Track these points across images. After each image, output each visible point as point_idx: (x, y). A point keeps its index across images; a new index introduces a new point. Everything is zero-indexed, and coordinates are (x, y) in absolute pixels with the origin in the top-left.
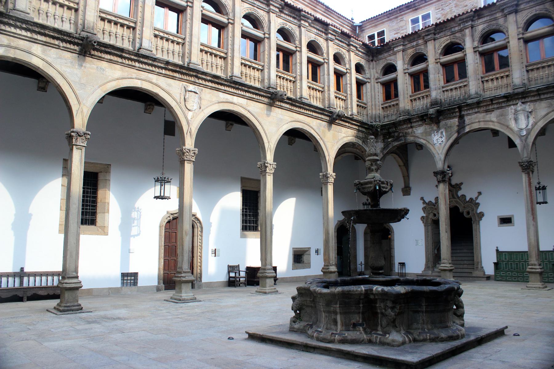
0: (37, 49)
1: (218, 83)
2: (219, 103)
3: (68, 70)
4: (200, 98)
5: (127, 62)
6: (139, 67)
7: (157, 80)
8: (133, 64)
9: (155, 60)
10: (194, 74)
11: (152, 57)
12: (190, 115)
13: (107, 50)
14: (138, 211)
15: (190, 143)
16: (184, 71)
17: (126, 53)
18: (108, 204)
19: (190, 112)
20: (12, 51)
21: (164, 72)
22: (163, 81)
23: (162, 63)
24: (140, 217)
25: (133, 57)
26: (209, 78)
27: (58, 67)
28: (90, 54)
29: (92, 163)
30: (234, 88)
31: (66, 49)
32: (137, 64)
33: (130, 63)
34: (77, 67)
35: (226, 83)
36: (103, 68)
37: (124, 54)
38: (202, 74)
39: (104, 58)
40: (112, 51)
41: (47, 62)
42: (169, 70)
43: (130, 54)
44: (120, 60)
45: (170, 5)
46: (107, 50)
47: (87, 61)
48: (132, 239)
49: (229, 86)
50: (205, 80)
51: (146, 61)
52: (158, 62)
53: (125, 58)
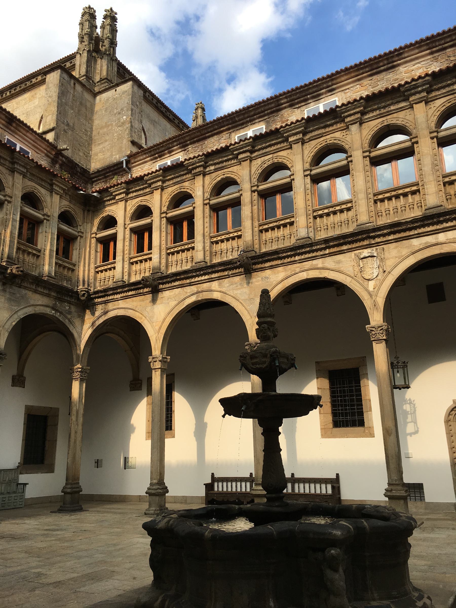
0: (215, 285)
1: (404, 231)
2: (413, 253)
3: (239, 292)
4: (382, 260)
5: (286, 260)
6: (300, 260)
7: (323, 263)
8: (293, 259)
9: (311, 245)
10: (364, 236)
11: (307, 244)
12: (371, 285)
13: (264, 259)
14: (410, 403)
15: (376, 318)
16: (349, 239)
17: (282, 253)
18: (370, 401)
19: (370, 282)
20: (201, 295)
21: (327, 251)
22: (329, 262)
23: (321, 244)
24: (415, 411)
25: (289, 253)
26: (385, 231)
27: (231, 293)
28: (253, 270)
29: (345, 360)
30: (433, 224)
31: (235, 275)
32: (297, 258)
33: (289, 260)
34: (245, 286)
35: (416, 225)
36: (267, 276)
37: (280, 255)
38: (374, 232)
39: (265, 267)
40: (269, 258)
41: (223, 292)
42: (333, 246)
43: (286, 252)
44: (279, 262)
45: (334, 173)
46: (264, 259)
47: (253, 276)
48: (408, 437)
49: (424, 226)
50: (384, 235)
51: (304, 250)
52: (317, 245)
53: (284, 258)
